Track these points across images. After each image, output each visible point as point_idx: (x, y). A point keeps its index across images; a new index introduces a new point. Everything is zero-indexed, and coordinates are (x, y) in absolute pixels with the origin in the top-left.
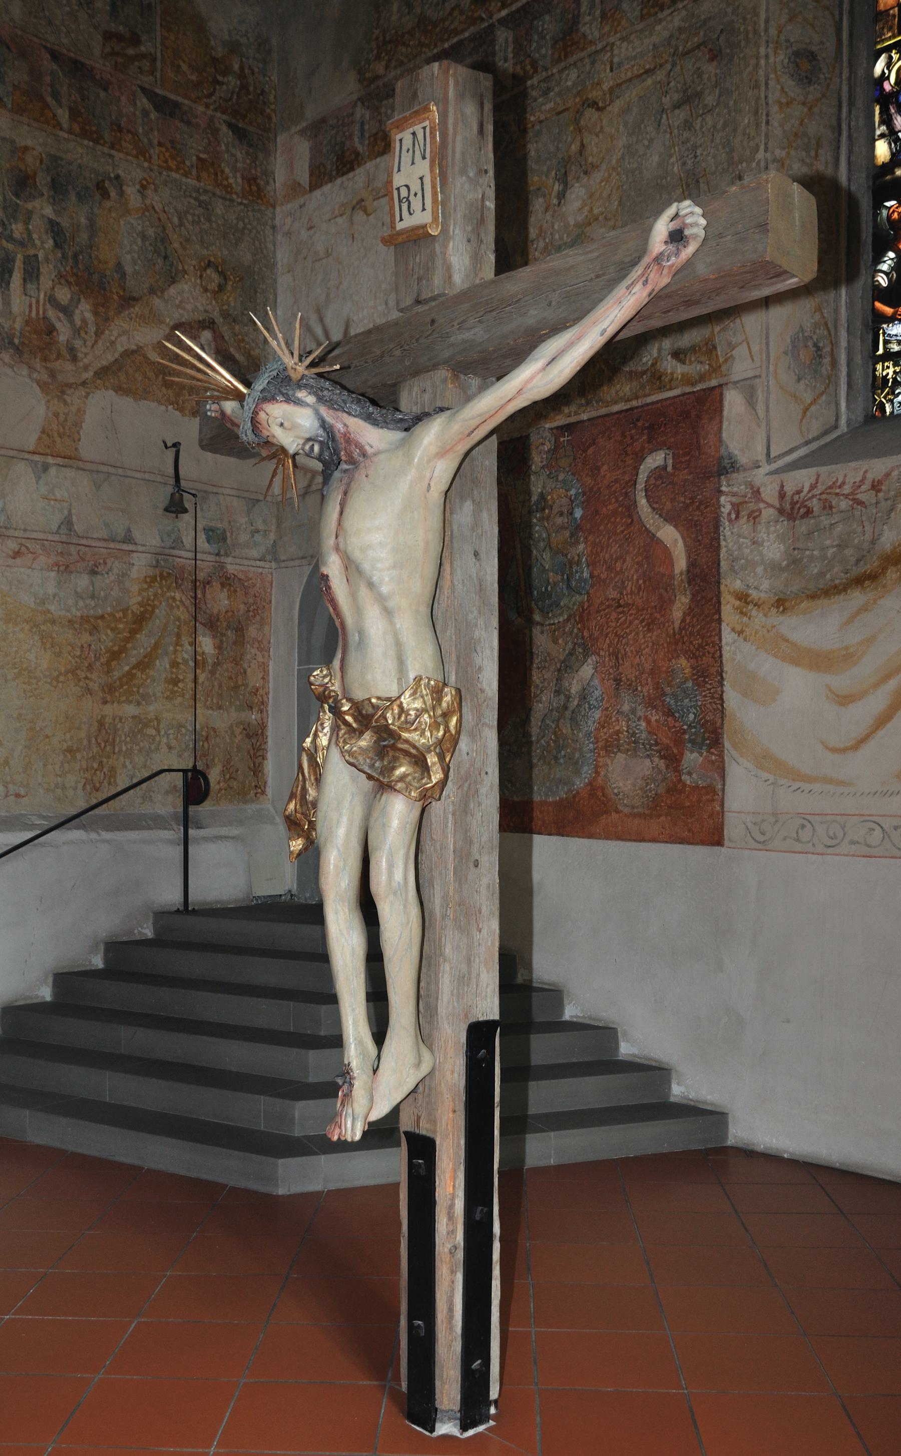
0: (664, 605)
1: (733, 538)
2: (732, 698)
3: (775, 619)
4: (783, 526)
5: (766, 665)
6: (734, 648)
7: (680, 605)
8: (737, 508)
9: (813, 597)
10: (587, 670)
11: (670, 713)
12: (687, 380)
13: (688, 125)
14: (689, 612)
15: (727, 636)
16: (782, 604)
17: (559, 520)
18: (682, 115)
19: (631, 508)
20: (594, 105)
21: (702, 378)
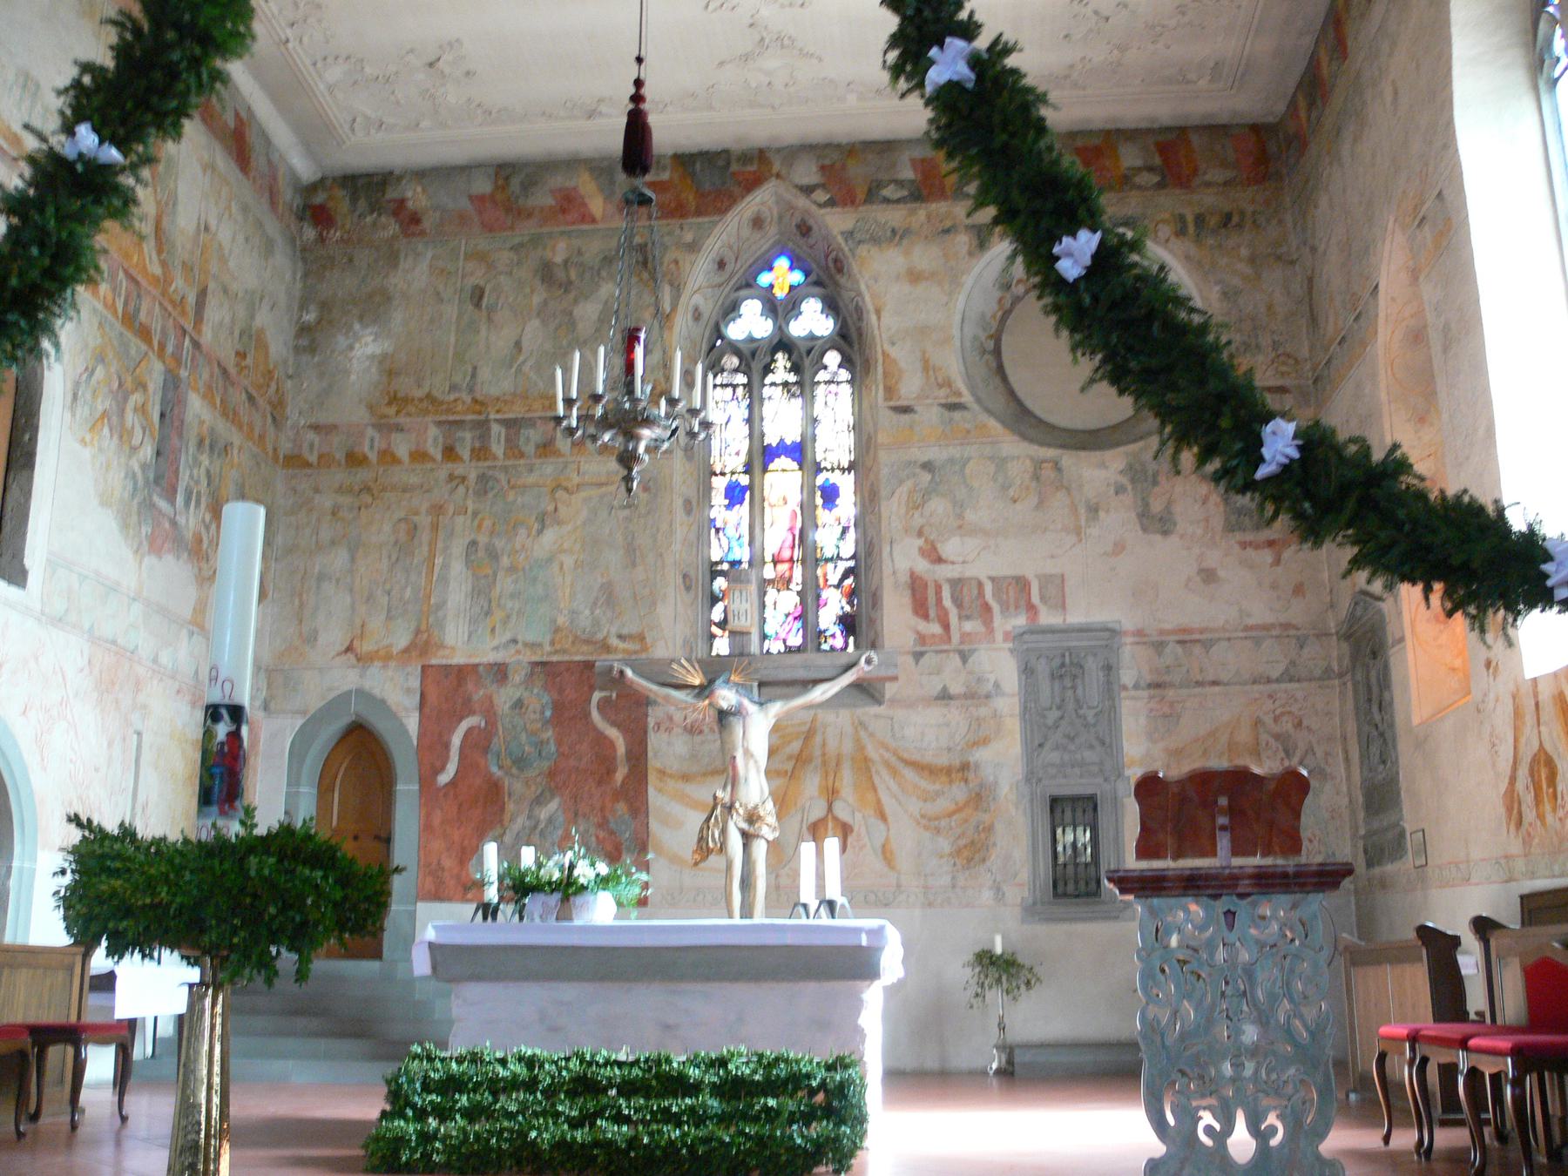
0: (610, 772)
1: (655, 741)
2: (654, 825)
3: (680, 785)
4: (686, 737)
5: (676, 809)
6: (654, 797)
7: (620, 774)
8: (658, 725)
9: (705, 775)
10: (553, 805)
11: (612, 833)
12: (625, 651)
13: (628, 519)
14: (627, 777)
15: (651, 791)
16: (686, 778)
17: (533, 716)
18: (626, 512)
19: (587, 715)
20: (566, 489)
21: (636, 652)
